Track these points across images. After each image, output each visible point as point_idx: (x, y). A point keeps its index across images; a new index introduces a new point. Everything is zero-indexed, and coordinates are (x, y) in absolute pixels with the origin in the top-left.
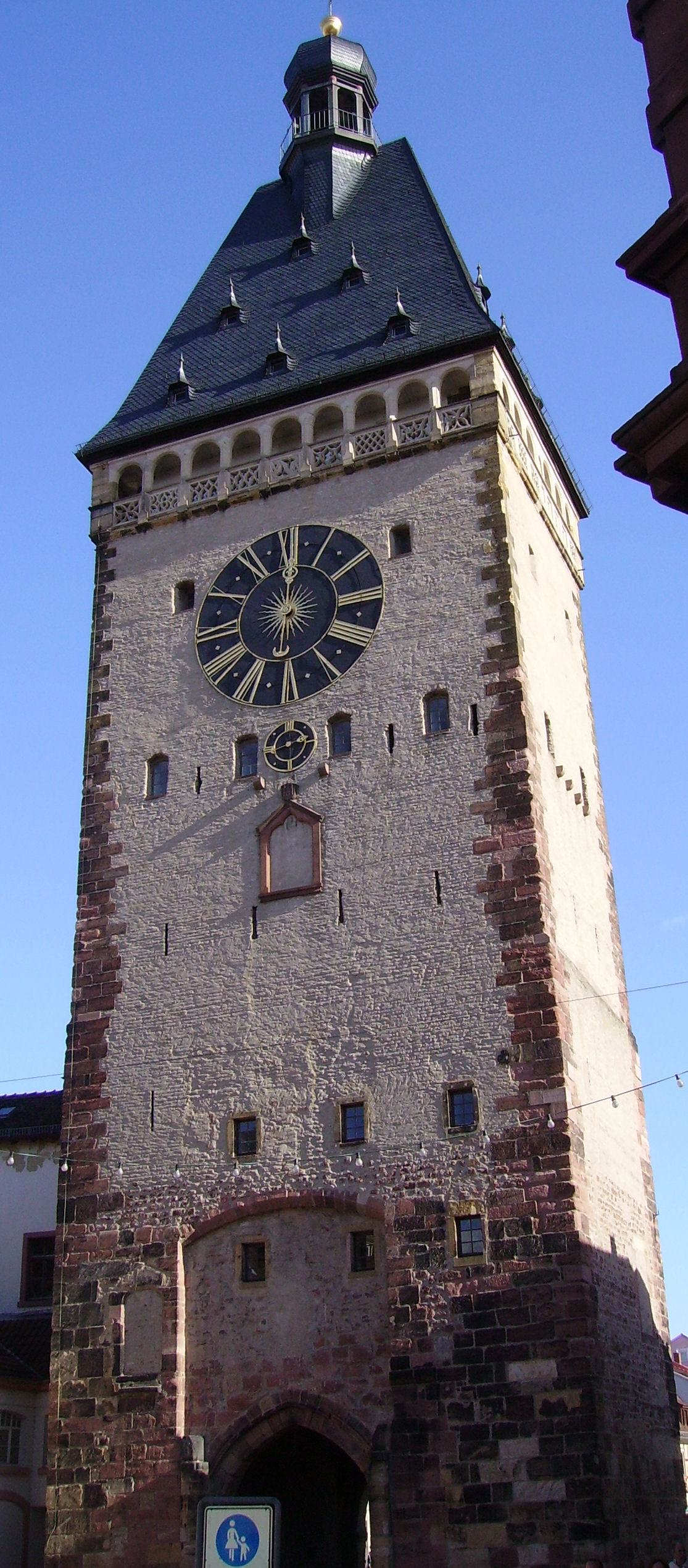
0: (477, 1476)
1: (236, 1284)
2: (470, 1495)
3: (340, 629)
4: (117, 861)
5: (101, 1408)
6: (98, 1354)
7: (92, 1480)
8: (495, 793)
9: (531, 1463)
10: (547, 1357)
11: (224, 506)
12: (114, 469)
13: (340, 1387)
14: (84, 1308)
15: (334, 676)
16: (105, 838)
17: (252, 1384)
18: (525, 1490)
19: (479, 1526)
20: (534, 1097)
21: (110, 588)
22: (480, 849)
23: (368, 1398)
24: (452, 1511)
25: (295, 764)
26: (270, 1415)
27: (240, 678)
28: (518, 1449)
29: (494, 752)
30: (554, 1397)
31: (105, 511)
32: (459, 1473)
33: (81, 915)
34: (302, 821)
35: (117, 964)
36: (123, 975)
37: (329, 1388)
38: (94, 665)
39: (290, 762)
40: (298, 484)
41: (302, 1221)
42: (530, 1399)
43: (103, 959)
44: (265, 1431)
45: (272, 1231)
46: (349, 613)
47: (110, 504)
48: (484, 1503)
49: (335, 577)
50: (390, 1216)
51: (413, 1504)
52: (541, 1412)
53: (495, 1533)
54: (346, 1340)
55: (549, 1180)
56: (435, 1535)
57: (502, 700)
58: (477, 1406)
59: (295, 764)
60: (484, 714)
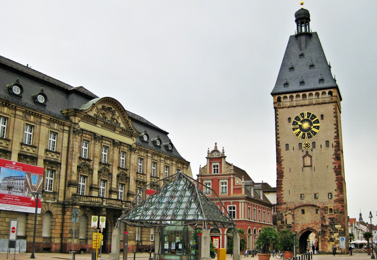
0: (331, 237)
1: (301, 214)
3: (314, 129)
4: (282, 159)
5: (284, 228)
10: (340, 225)
12: (277, 97)
13: (314, 227)
15: (313, 136)
16: (280, 155)
17: (303, 226)
18: (337, 239)
20: (339, 195)
21: (278, 116)
22: (333, 163)
23: (318, 228)
26: (305, 229)
28: (336, 235)
29: (335, 150)
30: (340, 229)
31: (276, 104)
32: (329, 237)
33: (277, 165)
34: (309, 156)
35: (283, 173)
36: (284, 174)
37: (313, 227)
39: (307, 148)
40: (307, 105)
41: (310, 207)
42: (338, 229)
43: (281, 172)
44: (305, 231)
47: (276, 103)
48: (332, 240)
49: (312, 121)
50: (321, 208)
51: (324, 240)
53: (333, 243)
54: (315, 221)
56: (326, 243)
57: (337, 143)
58: (331, 230)
60: (334, 145)
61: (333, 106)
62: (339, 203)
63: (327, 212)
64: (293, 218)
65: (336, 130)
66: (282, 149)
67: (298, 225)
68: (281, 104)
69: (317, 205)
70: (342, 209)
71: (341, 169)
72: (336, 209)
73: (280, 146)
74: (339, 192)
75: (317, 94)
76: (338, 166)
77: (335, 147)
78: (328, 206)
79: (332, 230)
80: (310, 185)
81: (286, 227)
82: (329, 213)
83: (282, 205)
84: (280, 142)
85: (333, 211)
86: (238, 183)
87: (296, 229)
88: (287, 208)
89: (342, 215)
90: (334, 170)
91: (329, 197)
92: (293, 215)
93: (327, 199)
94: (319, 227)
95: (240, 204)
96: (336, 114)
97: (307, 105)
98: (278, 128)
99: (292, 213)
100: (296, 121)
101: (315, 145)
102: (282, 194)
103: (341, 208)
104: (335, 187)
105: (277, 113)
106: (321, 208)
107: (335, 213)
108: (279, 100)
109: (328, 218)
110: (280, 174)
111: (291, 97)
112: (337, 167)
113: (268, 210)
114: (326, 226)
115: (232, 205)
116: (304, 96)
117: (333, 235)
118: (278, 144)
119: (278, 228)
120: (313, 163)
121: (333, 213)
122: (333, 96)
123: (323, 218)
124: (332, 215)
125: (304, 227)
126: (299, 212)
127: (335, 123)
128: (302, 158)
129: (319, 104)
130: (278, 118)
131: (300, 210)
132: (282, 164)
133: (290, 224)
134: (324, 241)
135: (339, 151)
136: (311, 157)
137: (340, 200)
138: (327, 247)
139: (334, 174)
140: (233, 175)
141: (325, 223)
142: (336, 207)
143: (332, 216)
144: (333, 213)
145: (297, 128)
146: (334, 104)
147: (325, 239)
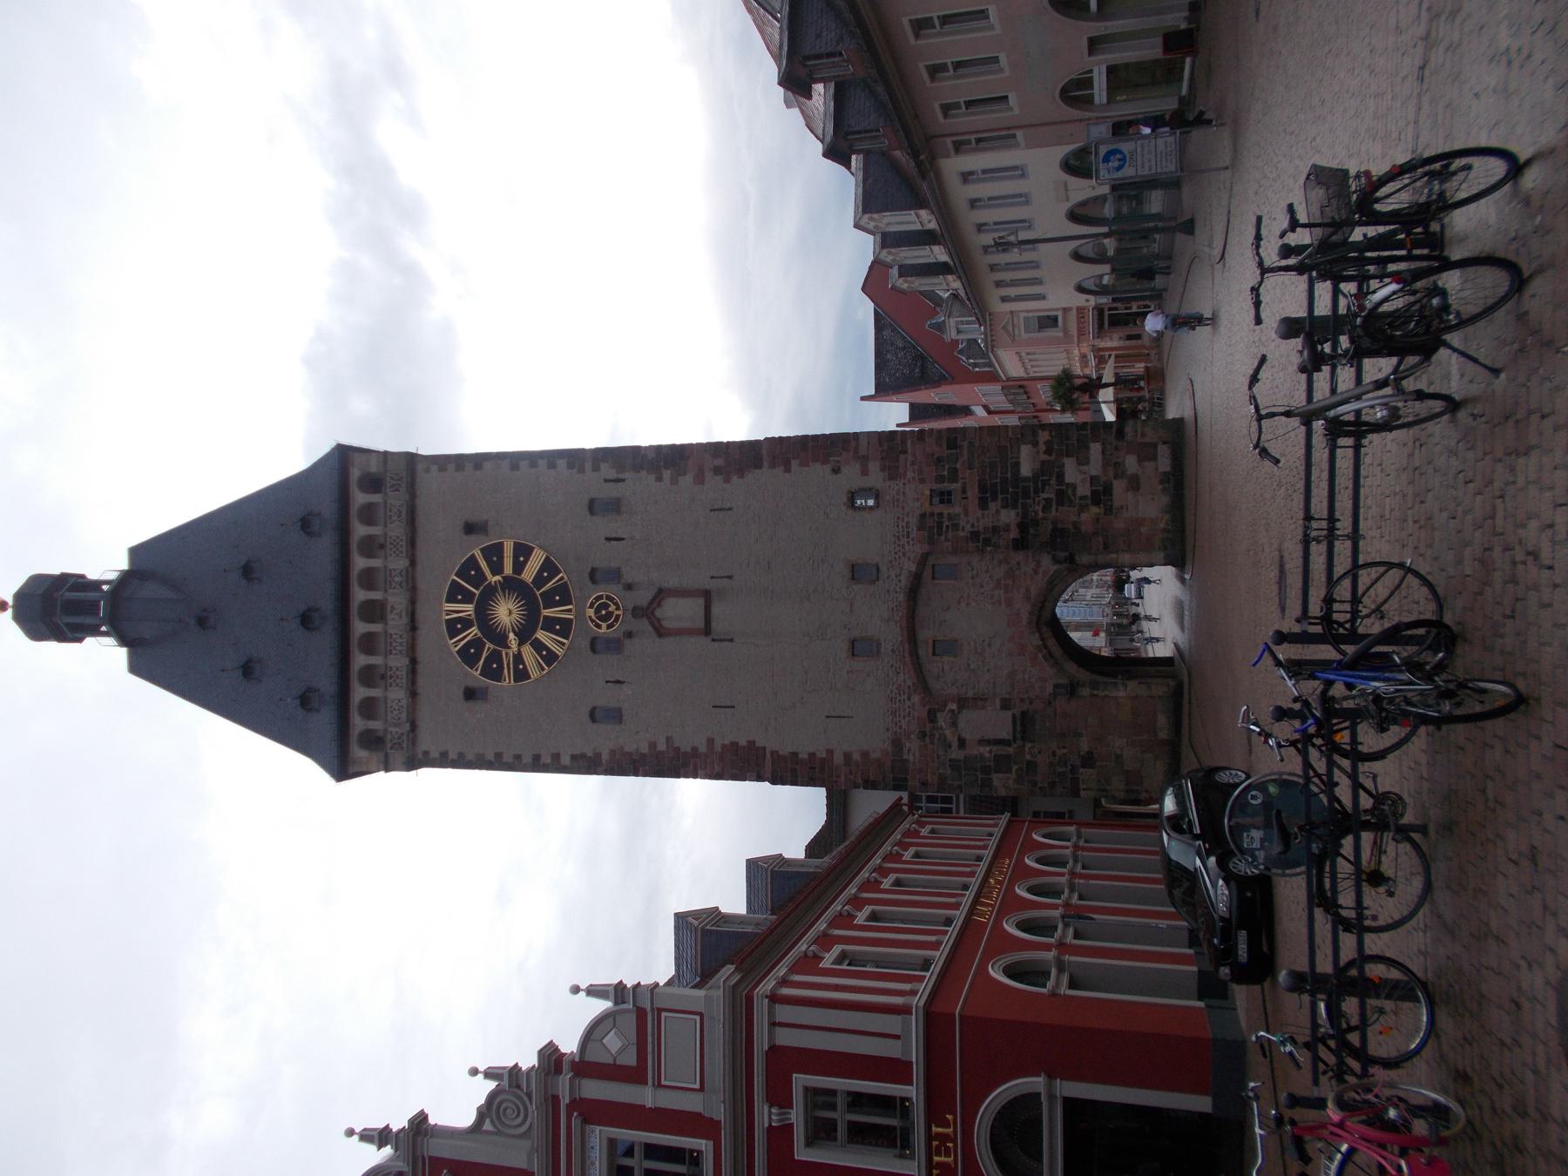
2: (1096, 503)
3: (528, 575)
4: (662, 747)
6: (997, 758)
7: (1078, 763)
9: (1080, 464)
12: (358, 752)
13: (1028, 590)
16: (643, 756)
18: (1095, 468)
20: (863, 452)
22: (700, 479)
26: (1042, 639)
29: (637, 468)
30: (1042, 448)
32: (1083, 508)
34: (659, 605)
35: (734, 744)
36: (743, 742)
42: (1043, 462)
44: (1051, 642)
45: (926, 634)
46: (519, 567)
48: (1101, 495)
50: (926, 548)
53: (1119, 487)
54: (998, 586)
58: (1044, 495)
62: (905, 452)
73: (598, 755)
78: (918, 512)
79: (1049, 494)
81: (1028, 745)
82: (957, 509)
85: (946, 486)
88: (923, 735)
90: (735, 479)
92: (963, 702)
95: (786, 1038)
99: (954, 706)
102: (847, 756)
104: (820, 471)
106: (926, 548)
107: (954, 476)
109: (979, 513)
112: (719, 462)
115: (796, 1116)
116: (374, 611)
117: (1074, 487)
123: (982, 540)
124: (964, 492)
126: (947, 668)
128: (668, 642)
129: (412, 543)
136: (661, 594)
138: (1139, 522)
141: (1007, 528)
142: (921, 472)
143: (973, 493)
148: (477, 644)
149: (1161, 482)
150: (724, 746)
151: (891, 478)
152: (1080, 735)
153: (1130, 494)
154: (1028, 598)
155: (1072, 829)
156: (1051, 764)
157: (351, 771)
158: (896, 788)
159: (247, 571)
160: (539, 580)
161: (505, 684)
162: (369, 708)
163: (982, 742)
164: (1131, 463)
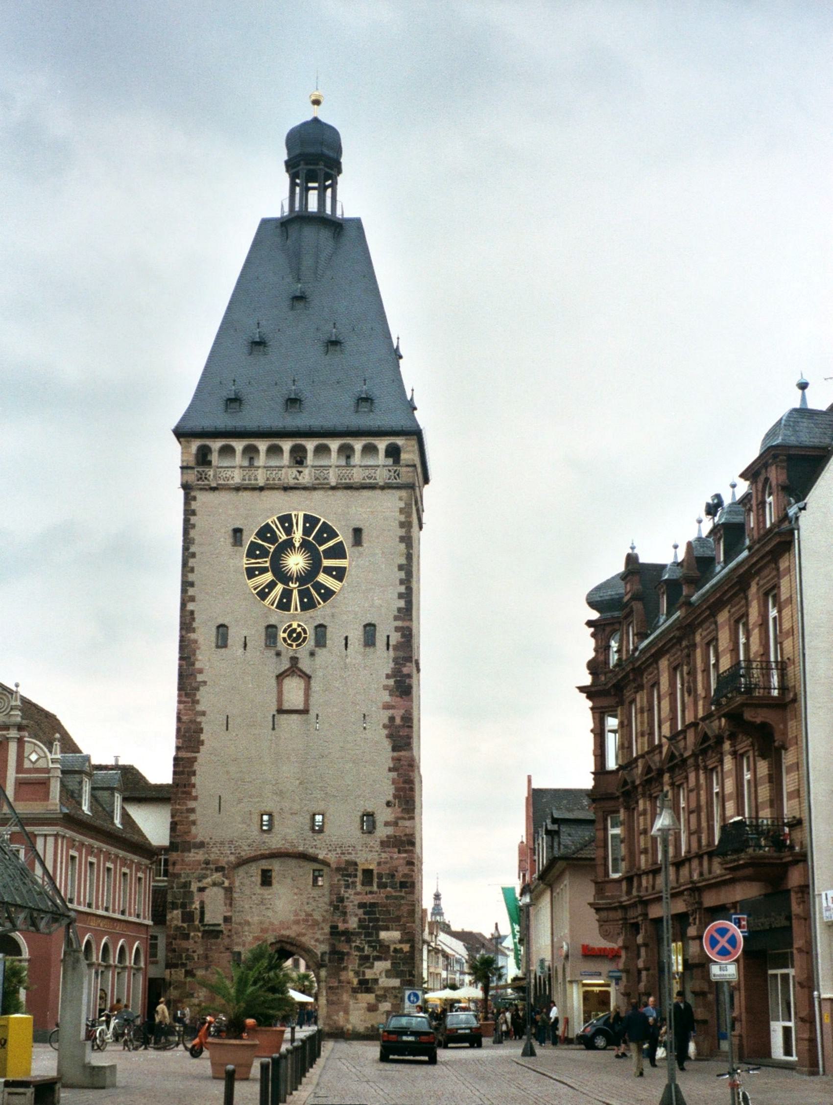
3: (322, 578)
4: (200, 678)
5: (193, 938)
7: (188, 968)
8: (395, 682)
9: (387, 971)
10: (396, 930)
11: (261, 489)
13: (304, 935)
14: (184, 892)
15: (319, 603)
16: (193, 664)
17: (263, 931)
18: (385, 982)
19: (364, 995)
20: (401, 823)
21: (193, 520)
22: (387, 707)
23: (317, 940)
24: (353, 988)
25: (297, 646)
27: (269, 593)
29: (396, 660)
30: (398, 946)
32: (357, 973)
33: (180, 702)
34: (300, 676)
35: (201, 730)
36: (203, 737)
37: (300, 934)
38: (185, 564)
39: (294, 644)
41: (293, 863)
42: (388, 947)
43: (193, 727)
45: (276, 866)
46: (328, 571)
48: (366, 986)
49: (322, 548)
50: (334, 866)
51: (336, 984)
52: (393, 952)
53: (370, 998)
55: (404, 858)
56: (345, 997)
57: (403, 636)
59: (297, 646)
61: (401, 499)
62: (399, 852)
63: (354, 883)
64: (228, 902)
65: (402, 589)
66: (201, 640)
67: (246, 928)
68: (211, 473)
69: (320, 857)
70: (406, 872)
71: (411, 727)
72: (385, 869)
73: (194, 630)
74: (400, 810)
75: (346, 451)
76: (402, 718)
77: (396, 648)
78: (358, 860)
79: (367, 950)
80: (298, 782)
81: (200, 934)
82: (359, 887)
83: (190, 851)
84: (196, 616)
85: (376, 880)
86: (37, 760)
87: (238, 944)
88: (207, 863)
89: (406, 893)
90: (386, 732)
91: (362, 828)
92: (229, 890)
93: (358, 833)
94: (321, 938)
95: (40, 842)
96: (409, 531)
97: (305, 488)
98: (191, 562)
99: (226, 884)
100: (260, 542)
101: (324, 636)
102: (193, 810)
103: (403, 870)
104: (388, 791)
105: (193, 508)
106: (334, 866)
107: (382, 886)
108: (203, 457)
109: (356, 903)
110: (189, 737)
111: (251, 452)
112: (398, 721)
113: (137, 870)
114: (348, 935)
118: (187, 622)
119: (168, 937)
120: (313, 700)
121: (375, 885)
122: (402, 462)
123: (338, 905)
125: (266, 935)
126: (253, 879)
127: (403, 561)
128: (273, 682)
129: (349, 487)
130: (194, 526)
131: (255, 870)
132: (198, 697)
133: (216, 922)
134: (337, 988)
135: (408, 664)
137: (404, 838)
138: (347, 1012)
139: (387, 745)
140: (20, 728)
142: (385, 863)
143: (369, 899)
144: (375, 888)
145: (263, 571)
146: (403, 493)
147: (340, 981)
148: (273, 539)
149: (372, 1026)
150: (200, 723)
151: (382, 843)
152: (207, 969)
153: (365, 1005)
154: (298, 935)
155: (142, 965)
156: (188, 950)
157: (181, 440)
158: (171, 843)
159: (334, 343)
160: (319, 586)
161: (245, 560)
162: (227, 451)
163: (202, 903)
164: (386, 1006)
